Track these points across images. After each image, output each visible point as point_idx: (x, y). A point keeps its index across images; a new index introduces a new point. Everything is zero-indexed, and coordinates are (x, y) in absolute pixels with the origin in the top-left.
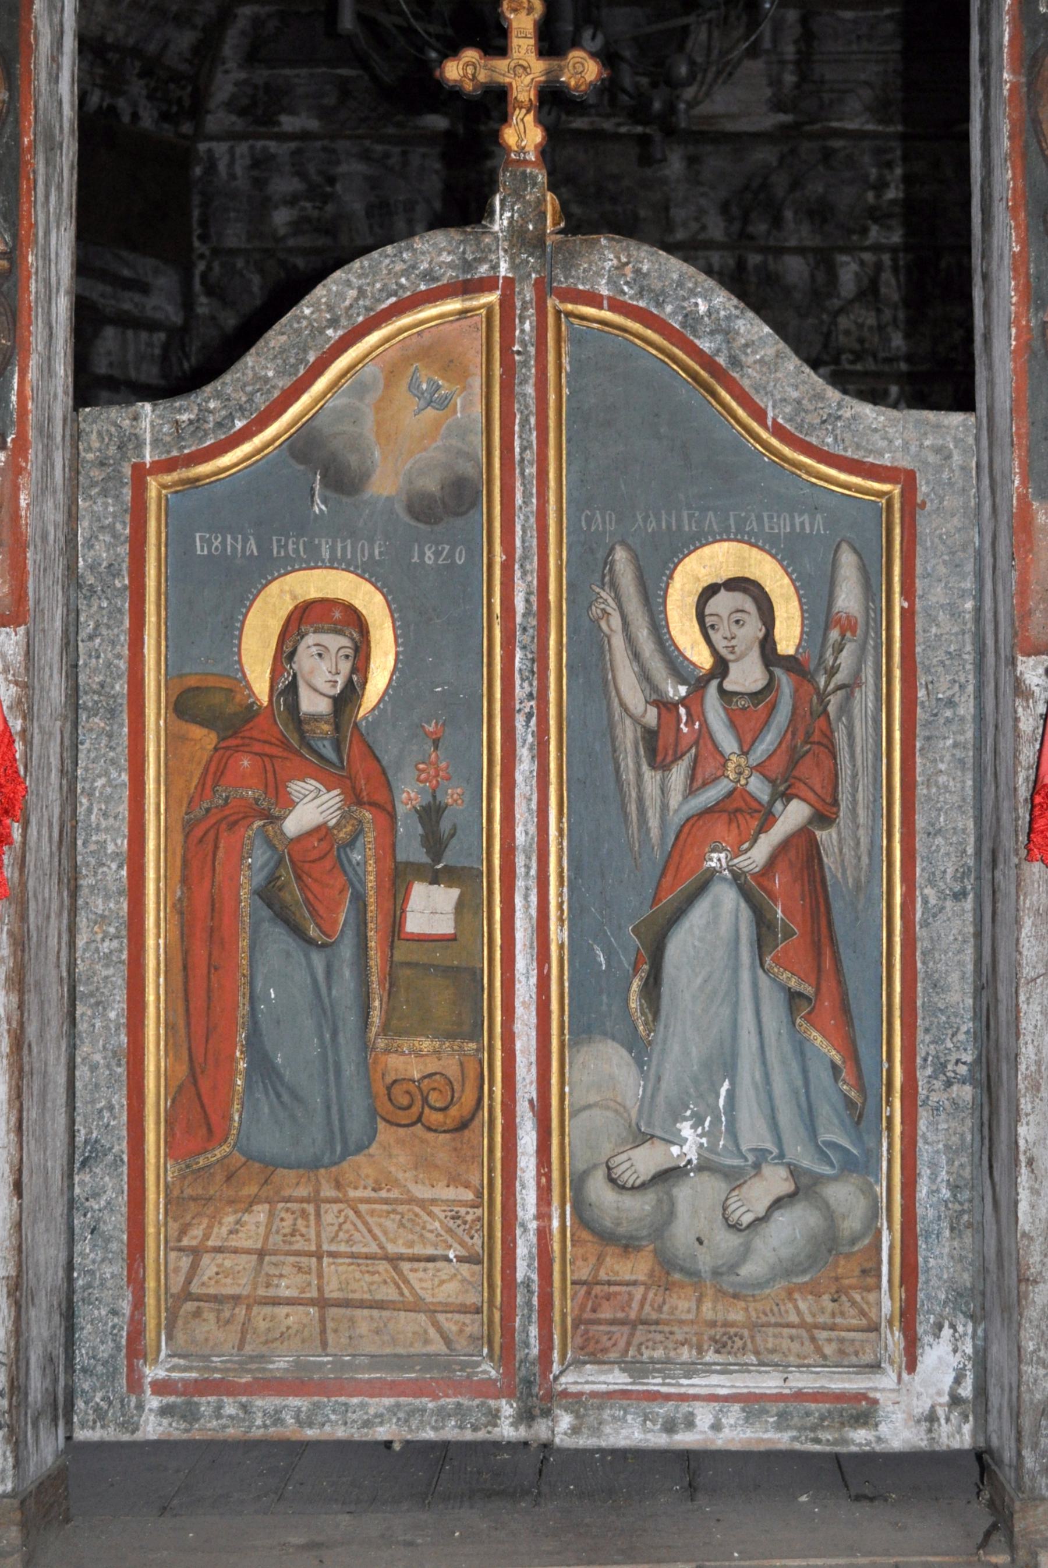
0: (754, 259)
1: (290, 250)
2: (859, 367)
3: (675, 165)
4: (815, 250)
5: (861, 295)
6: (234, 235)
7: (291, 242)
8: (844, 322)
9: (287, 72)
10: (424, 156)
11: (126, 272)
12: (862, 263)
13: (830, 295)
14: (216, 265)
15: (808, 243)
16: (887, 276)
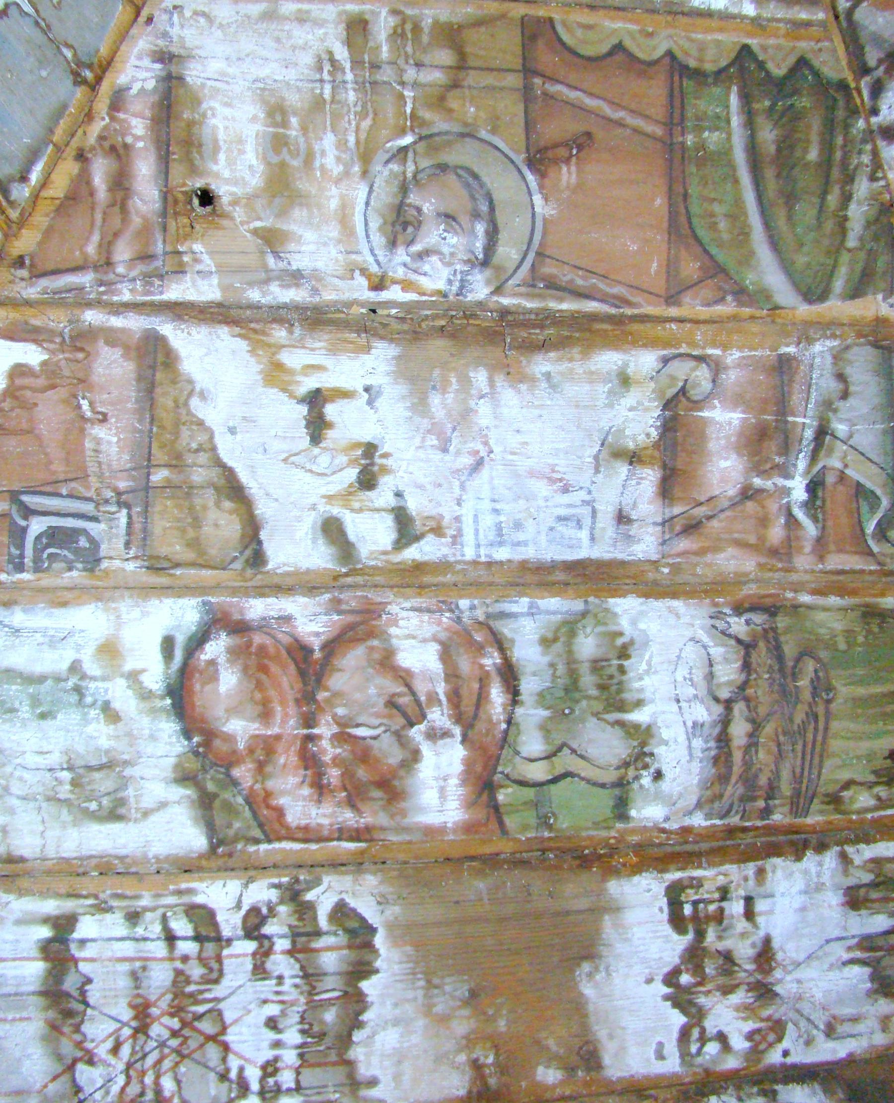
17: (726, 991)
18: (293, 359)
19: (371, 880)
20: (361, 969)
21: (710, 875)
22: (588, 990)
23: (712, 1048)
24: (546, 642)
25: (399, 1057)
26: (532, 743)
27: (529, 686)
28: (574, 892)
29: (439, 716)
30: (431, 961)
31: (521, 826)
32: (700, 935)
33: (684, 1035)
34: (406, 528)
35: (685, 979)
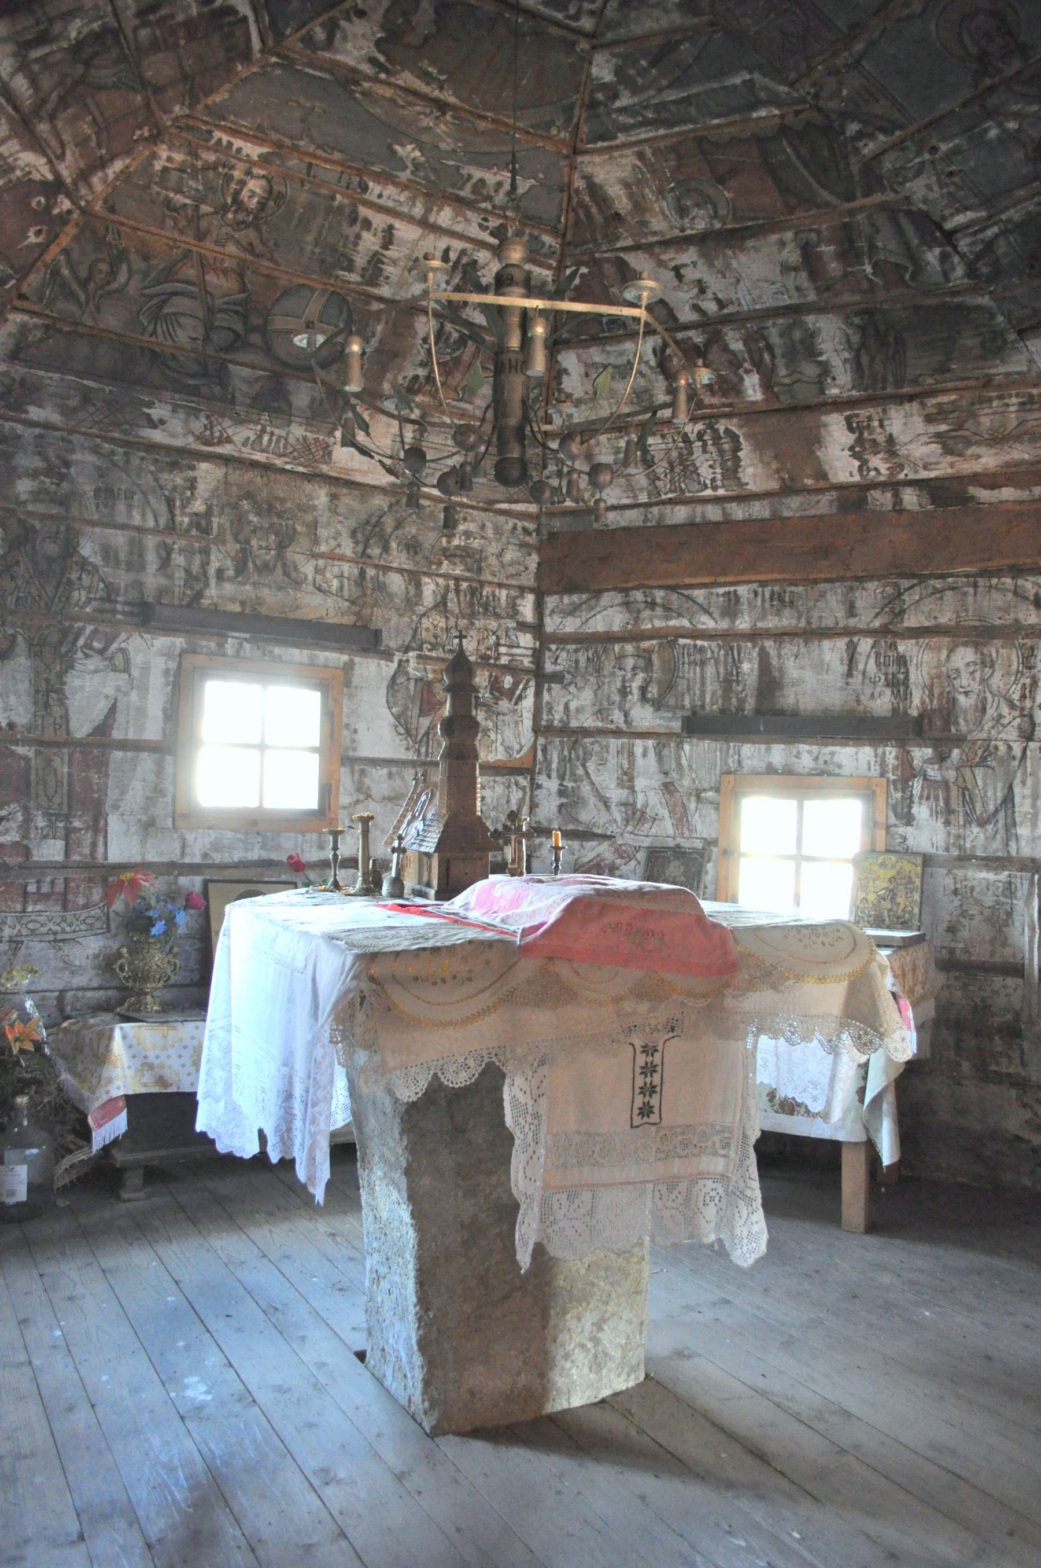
0: (371, 572)
1: (31, 514)
2: (434, 654)
4: (410, 572)
5: (436, 606)
7: (30, 507)
8: (426, 623)
9: (42, 373)
12: (437, 584)
13: (416, 604)
15: (405, 567)
16: (451, 595)
17: (876, 453)
18: (665, 257)
19: (735, 420)
20: (737, 448)
21: (863, 413)
22: (819, 453)
23: (873, 473)
24: (781, 336)
25: (754, 476)
26: (783, 371)
27: (778, 351)
28: (808, 419)
29: (747, 365)
30: (759, 446)
31: (786, 401)
32: (861, 434)
33: (860, 469)
34: (721, 304)
35: (857, 449)
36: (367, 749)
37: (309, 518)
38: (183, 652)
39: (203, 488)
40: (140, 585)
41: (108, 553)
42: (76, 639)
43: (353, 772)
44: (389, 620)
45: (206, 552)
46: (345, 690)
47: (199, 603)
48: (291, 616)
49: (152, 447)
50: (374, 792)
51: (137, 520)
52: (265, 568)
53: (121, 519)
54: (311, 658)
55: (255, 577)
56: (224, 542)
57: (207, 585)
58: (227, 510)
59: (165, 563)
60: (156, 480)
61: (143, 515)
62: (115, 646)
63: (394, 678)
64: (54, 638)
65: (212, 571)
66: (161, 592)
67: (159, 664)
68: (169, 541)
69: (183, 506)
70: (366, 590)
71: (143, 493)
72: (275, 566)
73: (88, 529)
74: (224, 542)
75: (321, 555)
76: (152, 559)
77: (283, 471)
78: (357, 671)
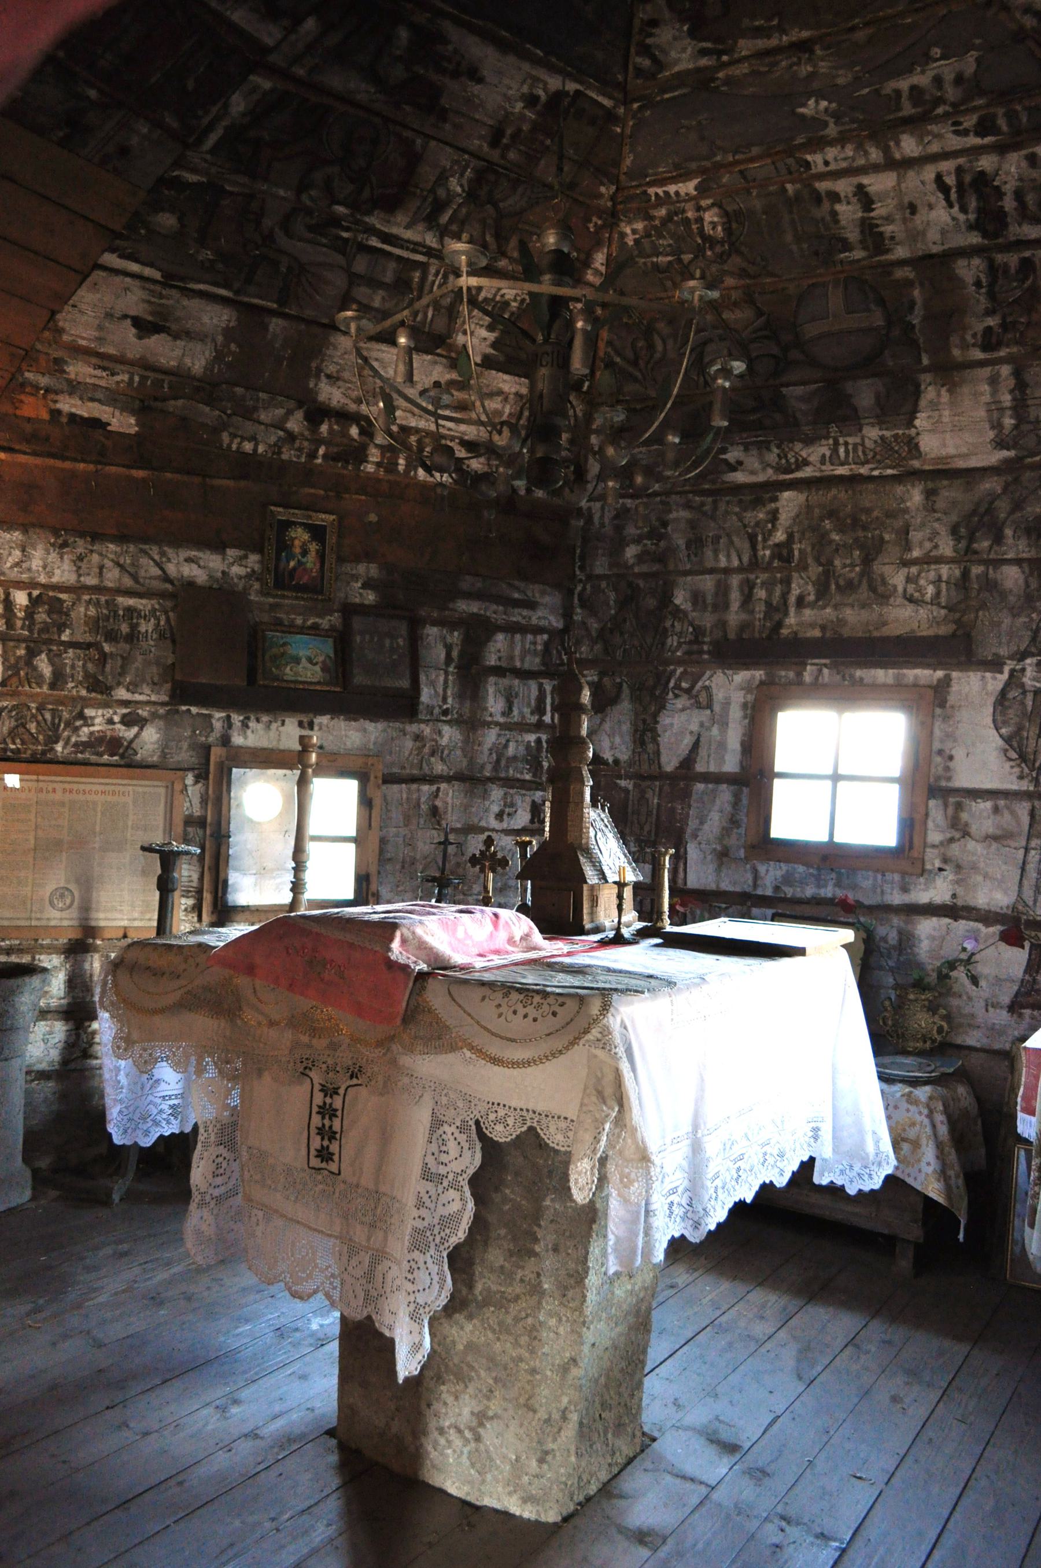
0: (976, 570)
3: (916, 496)
4: (1029, 561)
6: (601, 566)
7: (636, 570)
10: (728, 503)
11: (516, 595)
14: (588, 587)
36: (965, 778)
37: (899, 523)
38: (762, 683)
39: (785, 518)
40: (723, 624)
41: (697, 598)
42: (669, 681)
43: (946, 805)
44: (999, 624)
45: (787, 582)
46: (938, 711)
47: (778, 633)
48: (876, 634)
49: (738, 489)
50: (974, 829)
51: (723, 562)
52: (850, 587)
53: (709, 564)
54: (897, 677)
55: (838, 598)
56: (805, 568)
57: (786, 614)
58: (808, 535)
59: (747, 599)
60: (740, 520)
61: (728, 556)
62: (700, 684)
63: (1003, 693)
64: (651, 682)
65: (792, 600)
66: (743, 627)
67: (738, 698)
68: (752, 577)
69: (765, 540)
70: (969, 596)
71: (728, 535)
72: (860, 582)
73: (681, 580)
74: (805, 568)
75: (915, 562)
76: (735, 597)
77: (870, 479)
78: (955, 688)
